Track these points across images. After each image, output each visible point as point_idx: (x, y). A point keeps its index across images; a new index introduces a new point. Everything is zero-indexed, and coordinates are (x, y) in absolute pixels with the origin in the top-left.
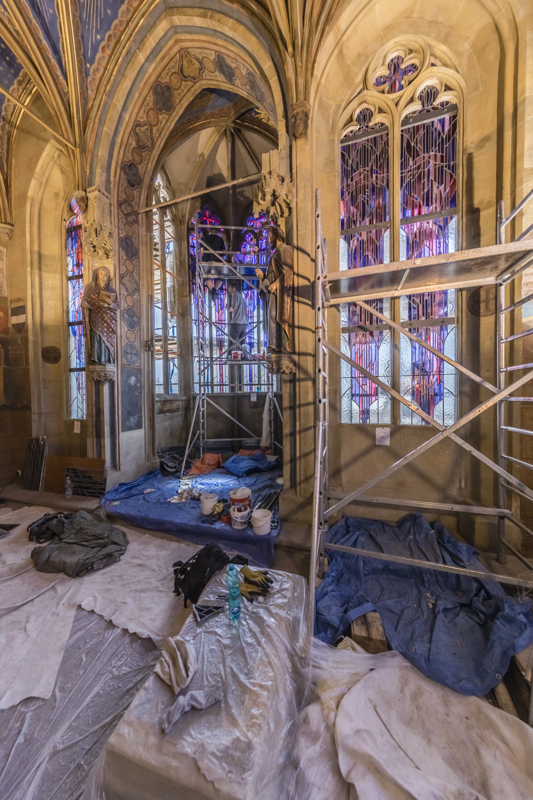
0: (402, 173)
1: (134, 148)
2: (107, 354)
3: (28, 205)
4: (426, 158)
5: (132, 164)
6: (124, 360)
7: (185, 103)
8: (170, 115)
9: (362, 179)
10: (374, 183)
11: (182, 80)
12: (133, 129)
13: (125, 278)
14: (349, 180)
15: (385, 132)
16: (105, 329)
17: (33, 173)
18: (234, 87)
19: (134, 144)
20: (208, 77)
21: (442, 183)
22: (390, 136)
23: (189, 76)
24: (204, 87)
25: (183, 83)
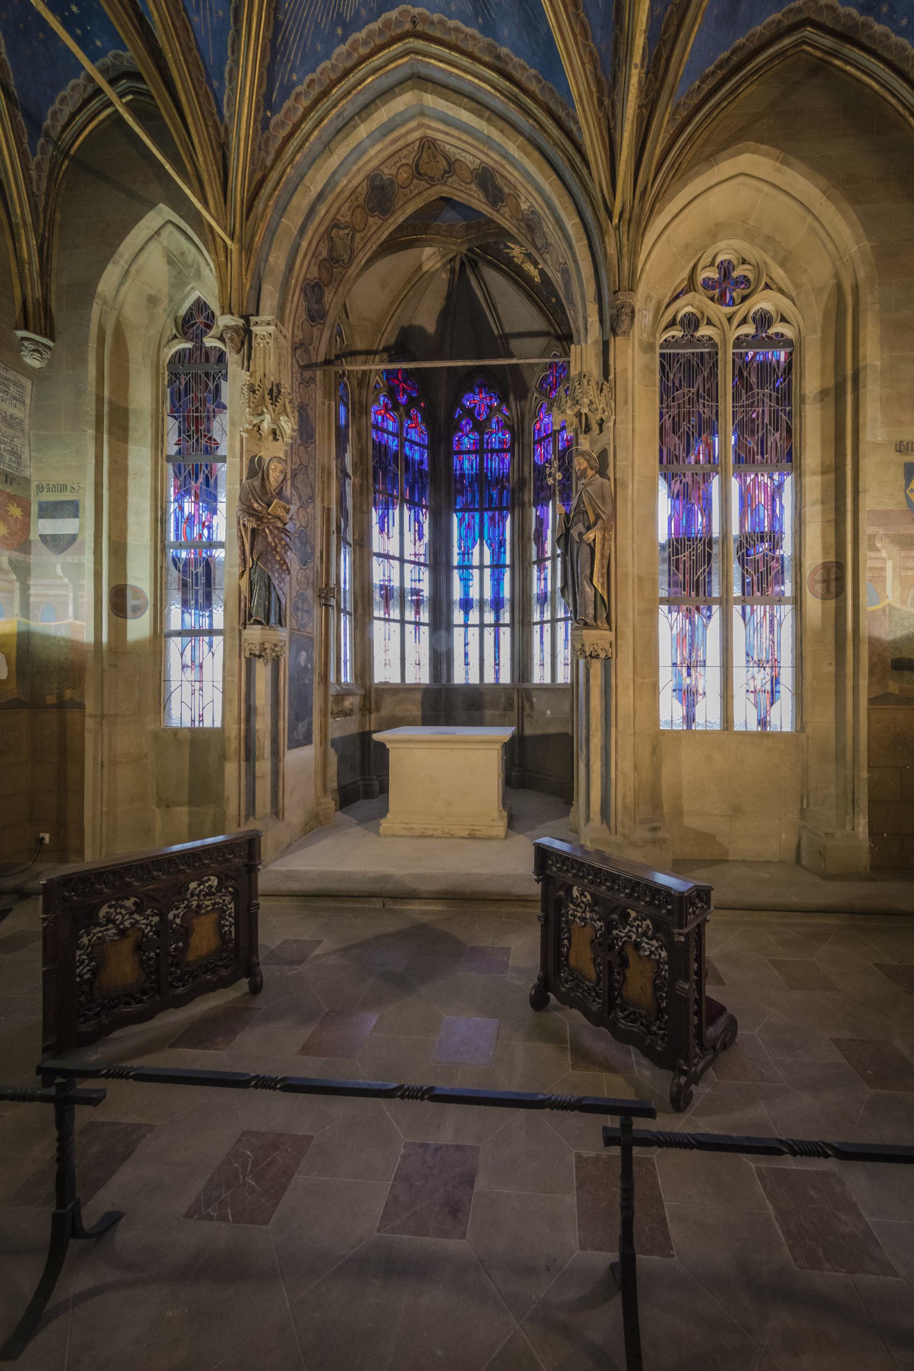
0: (733, 407)
1: (324, 260)
2: (277, 609)
3: (96, 309)
4: (761, 395)
5: (317, 284)
6: (294, 621)
7: (410, 209)
8: (385, 220)
9: (686, 403)
10: (701, 411)
11: (414, 176)
12: (328, 230)
13: (299, 477)
14: (670, 399)
15: (714, 350)
16: (277, 567)
17: (114, 253)
18: (495, 213)
19: (325, 254)
20: (455, 186)
21: (777, 431)
22: (720, 356)
23: (426, 174)
24: (444, 195)
25: (415, 181)
